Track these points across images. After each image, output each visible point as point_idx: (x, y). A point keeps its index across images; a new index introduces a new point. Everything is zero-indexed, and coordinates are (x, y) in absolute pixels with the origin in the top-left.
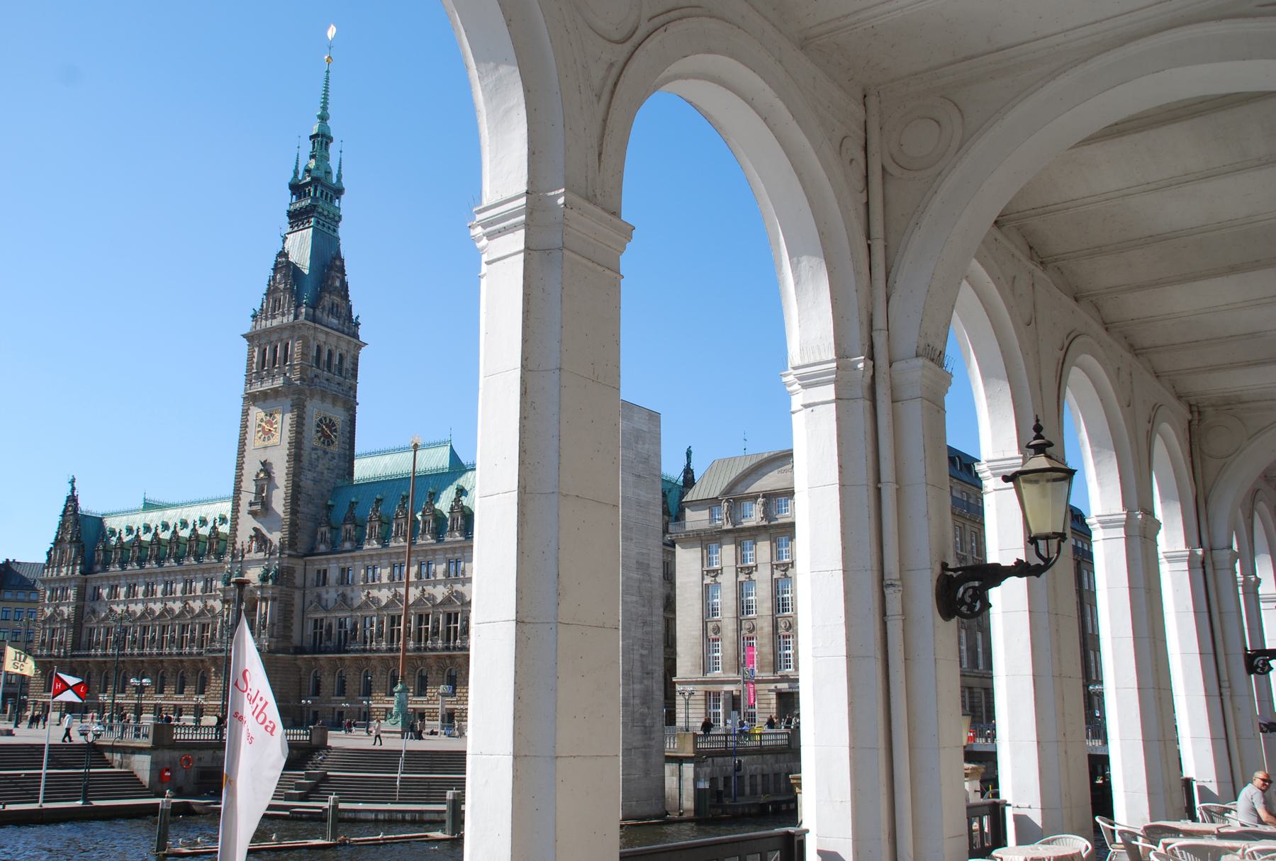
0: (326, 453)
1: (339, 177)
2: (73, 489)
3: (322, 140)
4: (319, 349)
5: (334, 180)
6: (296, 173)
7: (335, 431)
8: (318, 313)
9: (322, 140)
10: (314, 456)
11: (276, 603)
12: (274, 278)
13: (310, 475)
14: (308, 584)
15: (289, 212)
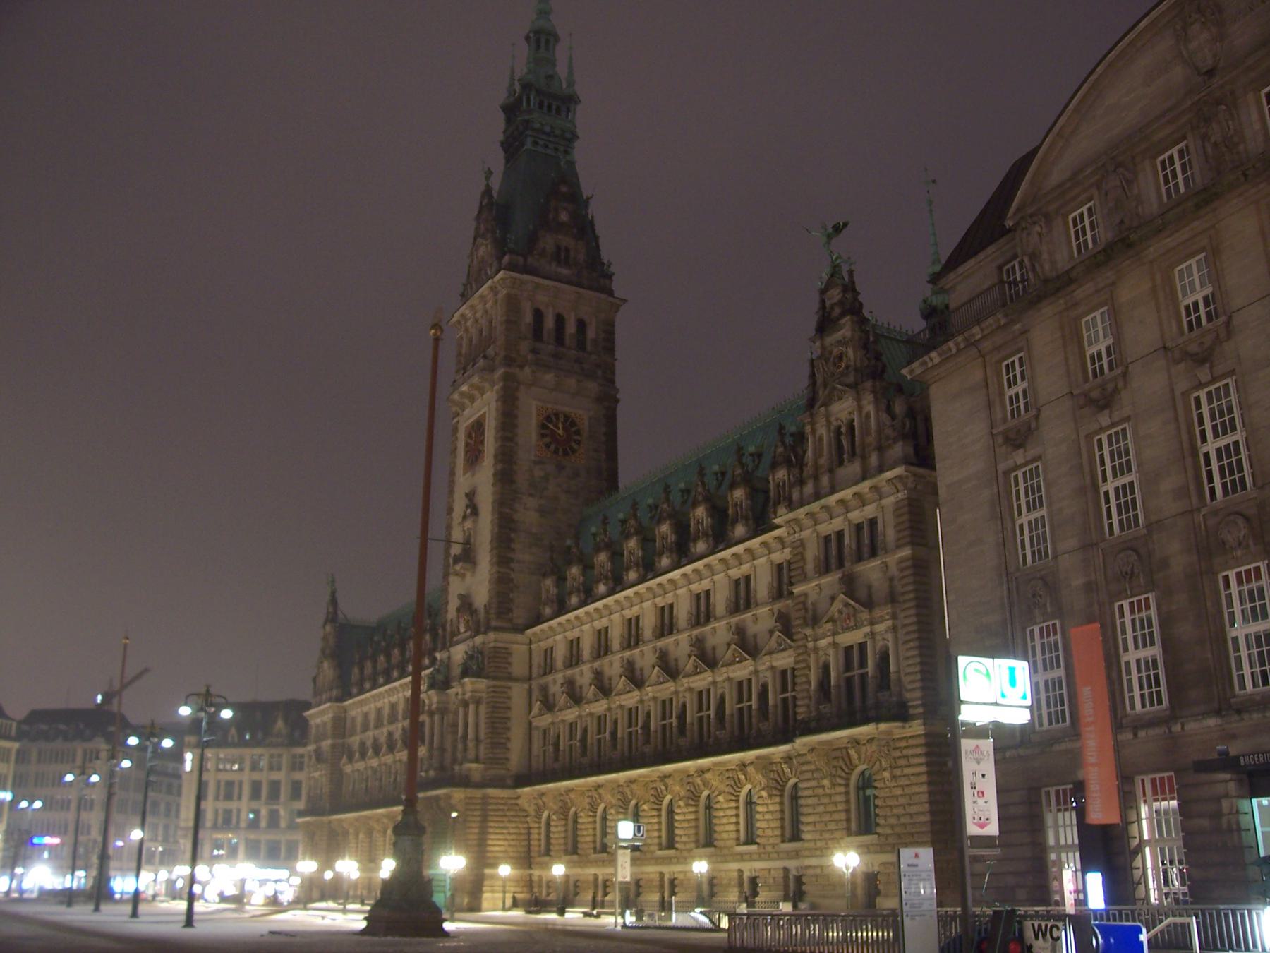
0: (560, 468)
1: (571, 83)
2: (333, 593)
3: (542, 39)
4: (538, 315)
5: (564, 86)
6: (511, 91)
7: (578, 433)
8: (530, 260)
9: (542, 39)
10: (538, 473)
11: (482, 709)
12: (477, 229)
13: (532, 503)
14: (534, 675)
15: (502, 144)
